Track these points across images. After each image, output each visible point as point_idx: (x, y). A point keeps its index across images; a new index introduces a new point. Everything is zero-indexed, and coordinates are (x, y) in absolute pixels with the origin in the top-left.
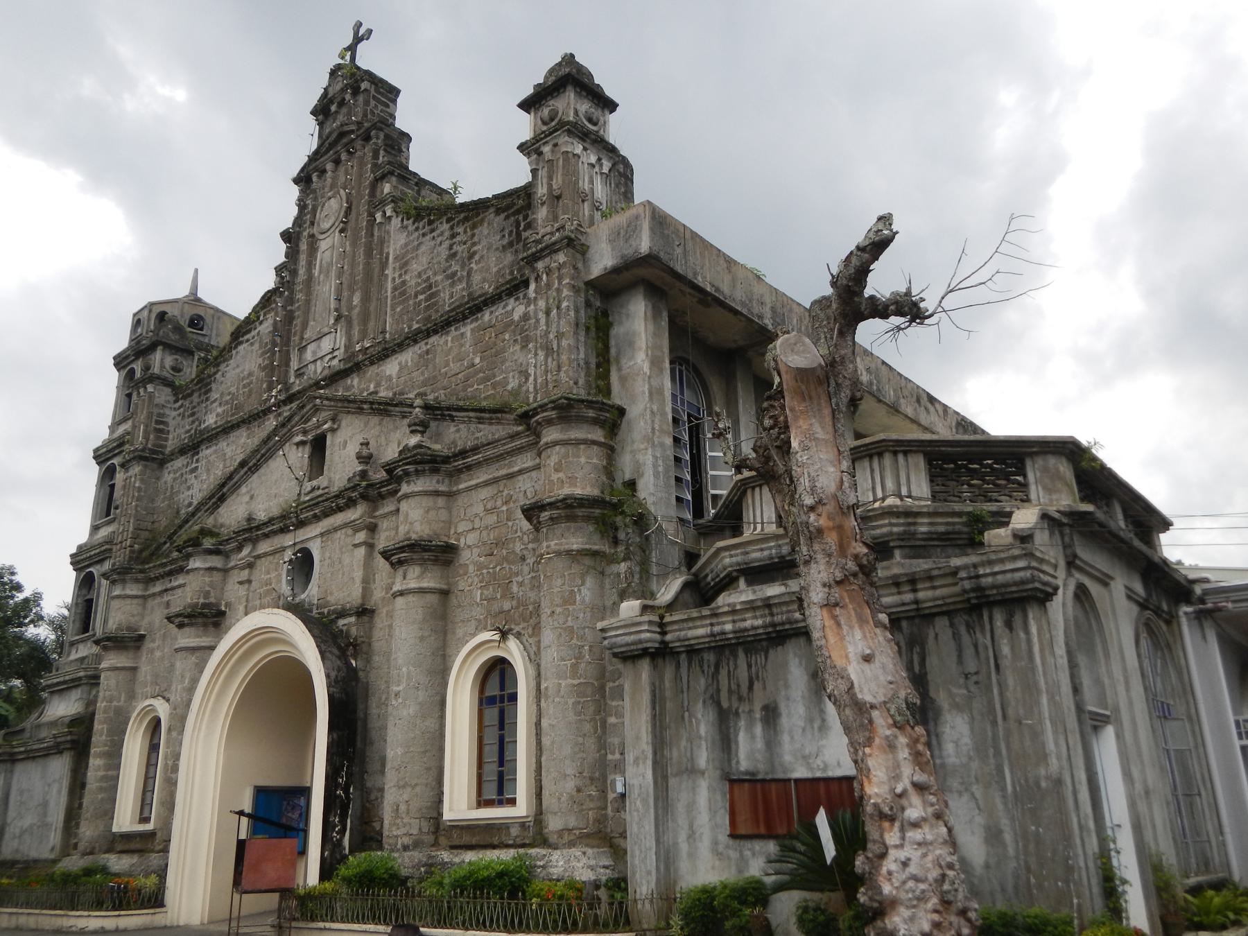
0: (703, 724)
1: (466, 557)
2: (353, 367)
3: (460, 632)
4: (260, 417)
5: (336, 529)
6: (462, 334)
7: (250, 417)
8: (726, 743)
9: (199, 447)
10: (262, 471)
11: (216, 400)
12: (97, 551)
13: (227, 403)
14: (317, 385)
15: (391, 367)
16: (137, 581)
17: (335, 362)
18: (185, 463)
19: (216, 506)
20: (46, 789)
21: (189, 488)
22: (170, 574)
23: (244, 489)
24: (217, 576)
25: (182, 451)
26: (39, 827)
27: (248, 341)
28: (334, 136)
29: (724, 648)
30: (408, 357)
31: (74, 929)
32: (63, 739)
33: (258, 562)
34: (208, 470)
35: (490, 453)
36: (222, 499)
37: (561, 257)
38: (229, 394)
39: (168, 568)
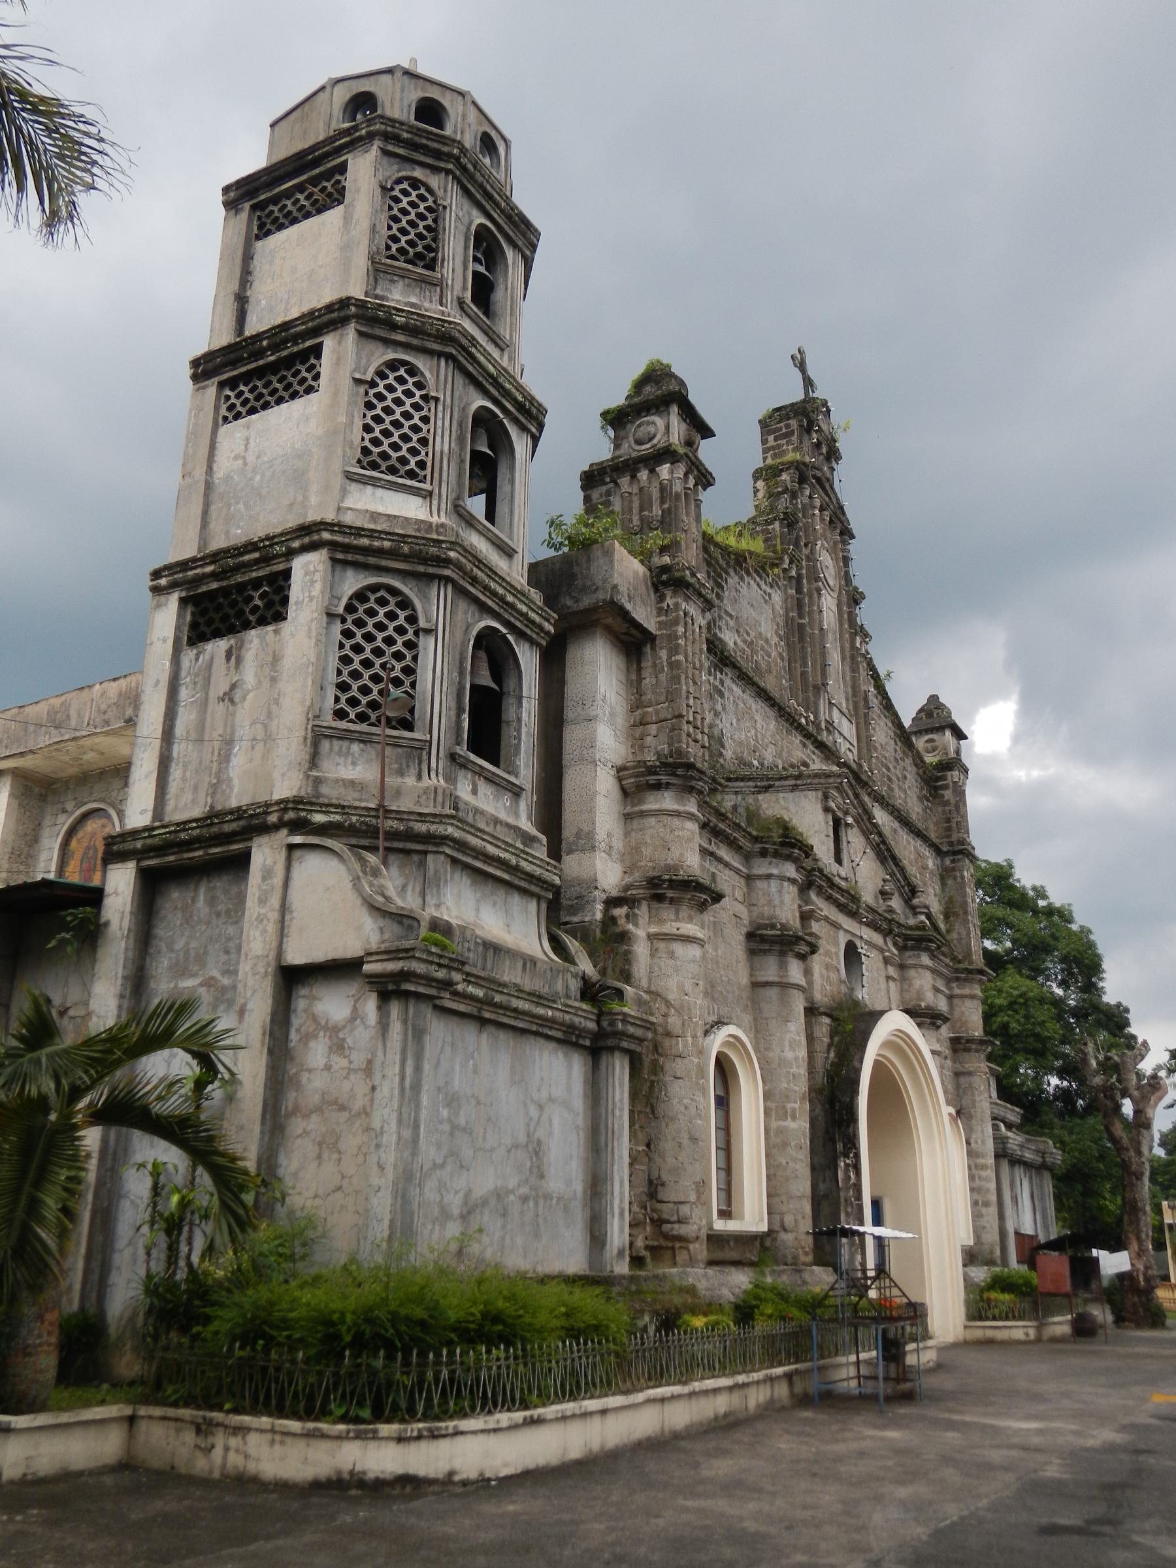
4: (791, 724)
6: (909, 843)
7: (789, 714)
9: (726, 665)
11: (731, 616)
12: (537, 619)
13: (745, 641)
20: (534, 1112)
26: (525, 1199)
27: (758, 585)
28: (819, 474)
31: (931, 1364)
32: (639, 1032)
36: (767, 789)
38: (748, 634)
39: (721, 826)
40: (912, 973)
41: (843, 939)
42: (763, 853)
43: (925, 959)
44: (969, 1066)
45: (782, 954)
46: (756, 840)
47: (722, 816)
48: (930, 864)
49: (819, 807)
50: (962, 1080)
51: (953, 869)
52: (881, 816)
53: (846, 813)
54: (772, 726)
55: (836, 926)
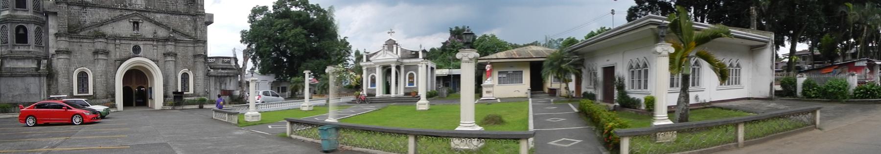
0: (218, 84)
1: (178, 56)
2: (146, 10)
3: (177, 68)
5: (147, 44)
8: (221, 86)
10: (116, 23)
14: (137, 10)
15: (158, 16)
16: (68, 37)
17: (142, 7)
18: (80, 9)
19: (99, 26)
21: (83, 17)
22: (82, 38)
23: (109, 25)
24: (106, 44)
25: (78, 5)
29: (221, 77)
30: (163, 15)
33: (121, 45)
34: (92, 15)
35: (184, 42)
36: (102, 25)
37: (203, 17)
40: (167, 46)
41: (132, 46)
42: (95, 38)
43: (170, 43)
44: (197, 60)
45: (98, 54)
46: (93, 36)
47: (81, 36)
48: (189, 19)
49: (128, 22)
50: (196, 63)
51: (196, 19)
52: (159, 17)
53: (139, 20)
54: (107, 12)
55: (131, 44)
